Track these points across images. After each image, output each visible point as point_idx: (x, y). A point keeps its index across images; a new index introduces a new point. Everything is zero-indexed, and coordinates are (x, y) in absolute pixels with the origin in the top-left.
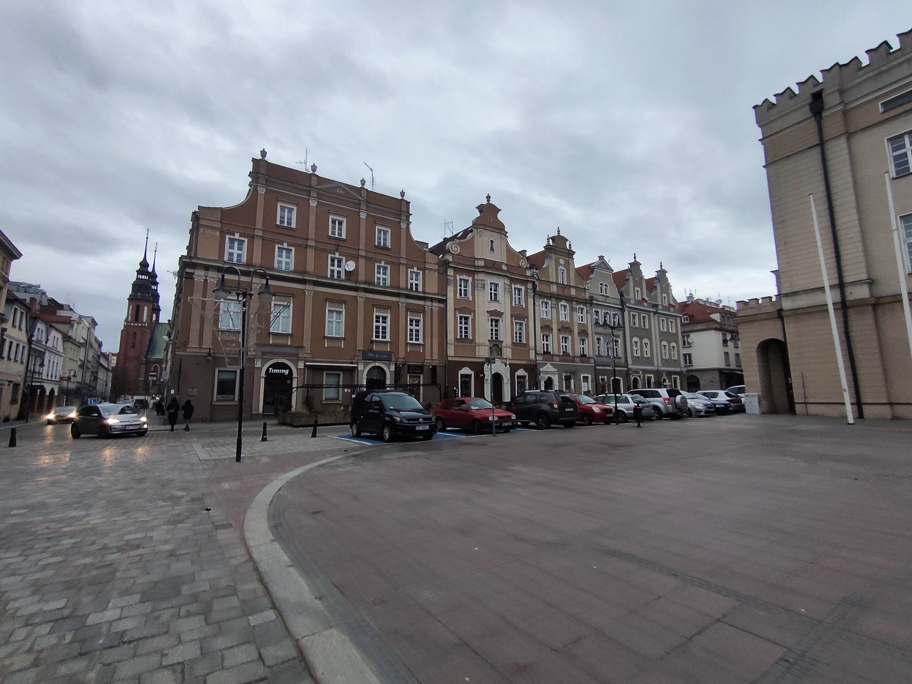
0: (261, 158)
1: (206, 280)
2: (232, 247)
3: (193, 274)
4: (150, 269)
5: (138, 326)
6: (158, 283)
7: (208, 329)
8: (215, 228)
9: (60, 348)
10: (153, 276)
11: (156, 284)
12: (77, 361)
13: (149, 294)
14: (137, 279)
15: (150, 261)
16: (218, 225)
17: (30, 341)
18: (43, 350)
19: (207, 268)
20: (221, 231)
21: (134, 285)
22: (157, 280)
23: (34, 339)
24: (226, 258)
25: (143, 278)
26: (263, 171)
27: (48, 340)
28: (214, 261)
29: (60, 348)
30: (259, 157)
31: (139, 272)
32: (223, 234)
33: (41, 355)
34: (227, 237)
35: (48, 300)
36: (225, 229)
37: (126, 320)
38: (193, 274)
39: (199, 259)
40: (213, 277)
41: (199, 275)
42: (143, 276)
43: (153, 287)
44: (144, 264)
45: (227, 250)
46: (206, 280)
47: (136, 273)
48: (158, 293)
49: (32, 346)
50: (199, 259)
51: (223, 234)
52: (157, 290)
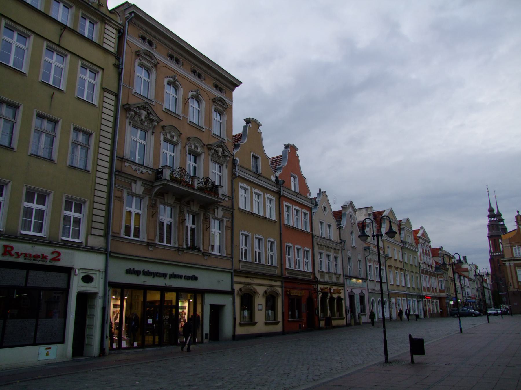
0: (517, 214)
1: (510, 265)
2: (516, 251)
3: (505, 263)
4: (495, 212)
5: (499, 255)
6: (503, 219)
7: (515, 281)
8: (508, 246)
9: (469, 285)
10: (499, 215)
11: (502, 220)
12: (475, 289)
13: (499, 231)
14: (490, 221)
15: (494, 207)
16: (509, 245)
17: (461, 285)
18: (464, 287)
19: (509, 261)
20: (511, 246)
21: (489, 226)
22: (503, 217)
23: (462, 284)
24: (515, 255)
25: (493, 220)
26: (519, 219)
27: (465, 283)
28: (511, 258)
29: (469, 285)
30: (517, 214)
31: (490, 216)
32: (511, 247)
33: (465, 289)
34: (513, 248)
35: (457, 260)
36: (512, 245)
37: (490, 251)
38: (505, 263)
39: (506, 258)
40: (512, 263)
41: (507, 264)
42: (492, 218)
43: (501, 223)
44: (491, 210)
45: (514, 252)
46: (510, 265)
47: (488, 217)
48: (505, 227)
49: (462, 287)
50: (506, 258)
51: (511, 247)
52: (504, 225)
